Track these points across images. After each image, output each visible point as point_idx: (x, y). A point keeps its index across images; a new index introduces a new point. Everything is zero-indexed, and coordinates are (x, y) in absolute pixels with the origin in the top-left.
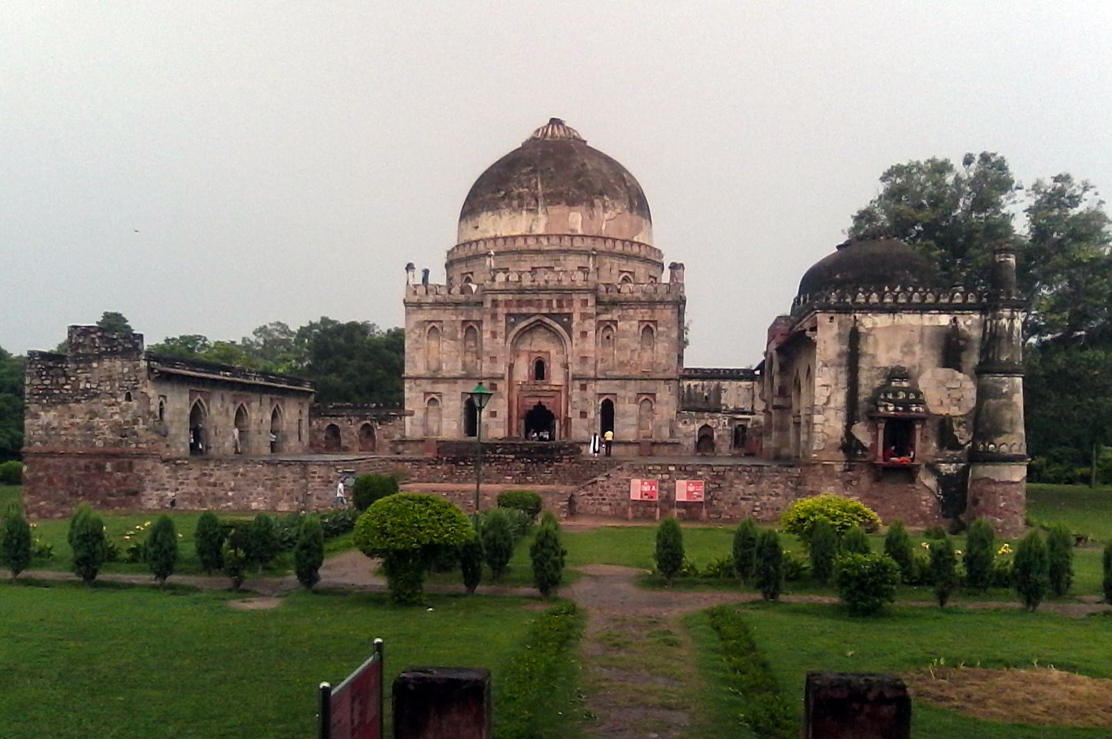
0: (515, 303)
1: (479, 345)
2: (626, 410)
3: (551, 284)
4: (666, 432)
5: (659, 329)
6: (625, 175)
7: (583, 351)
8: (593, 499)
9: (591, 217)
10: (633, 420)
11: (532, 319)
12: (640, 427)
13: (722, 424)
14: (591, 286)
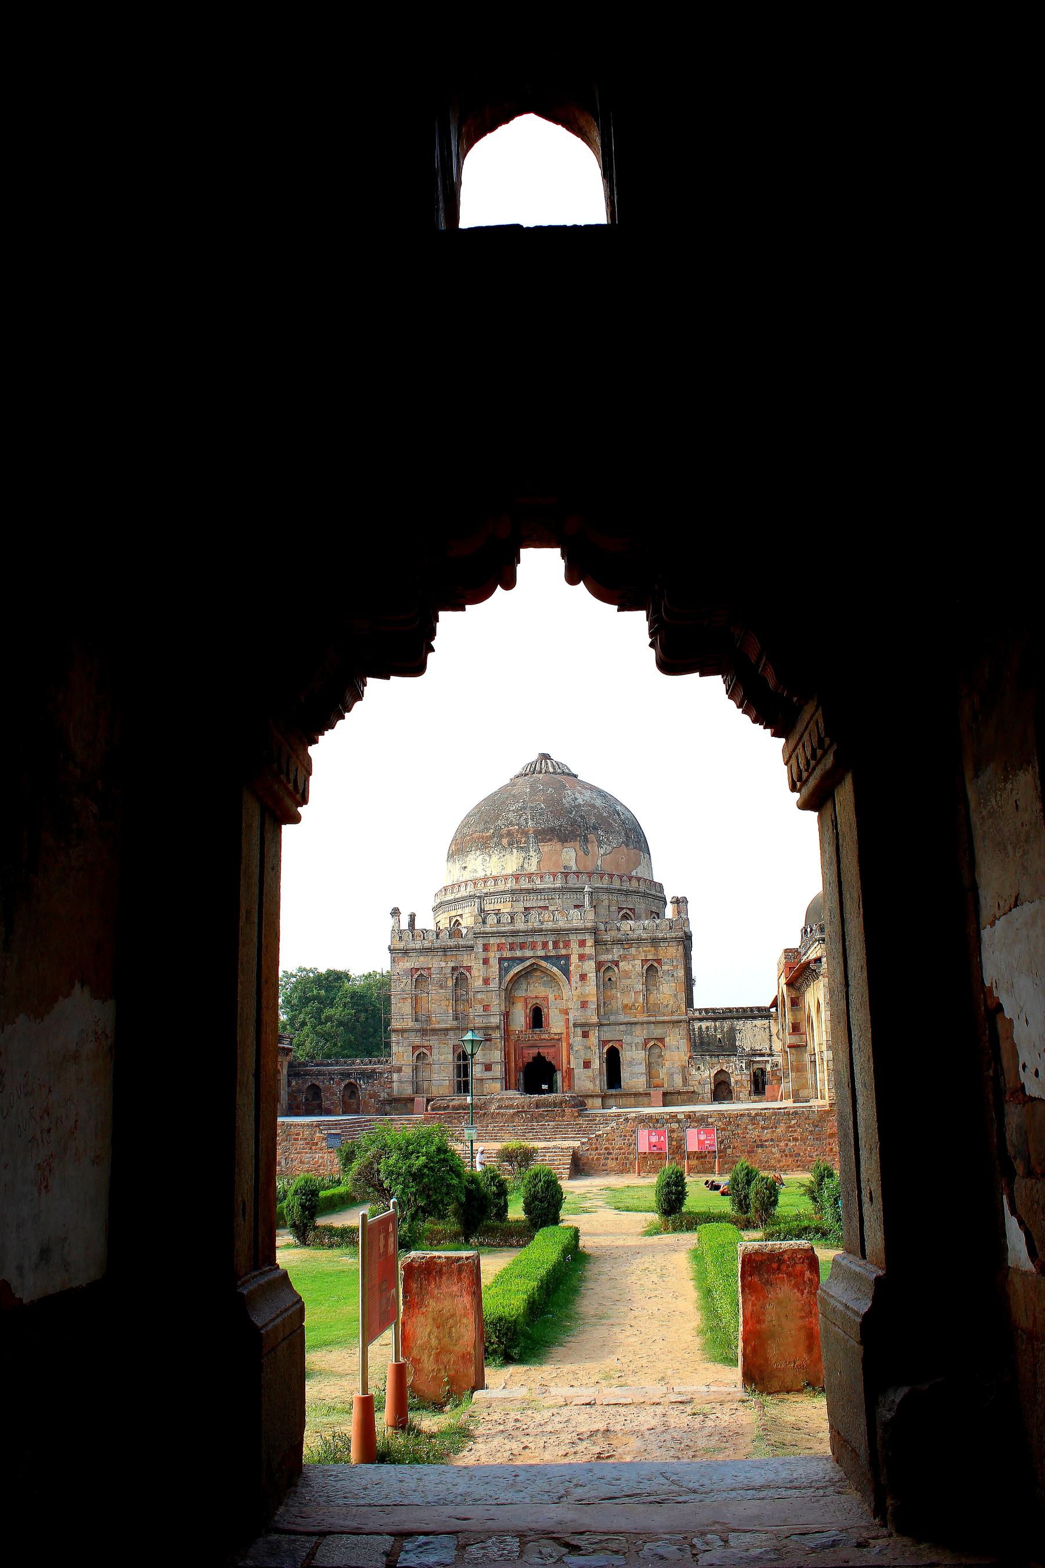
1: (471, 994)
3: (549, 925)
4: (678, 1080)
5: (665, 968)
6: (618, 808)
8: (599, 1154)
9: (586, 853)
10: (642, 1069)
11: (528, 963)
12: (650, 1074)
14: (589, 925)
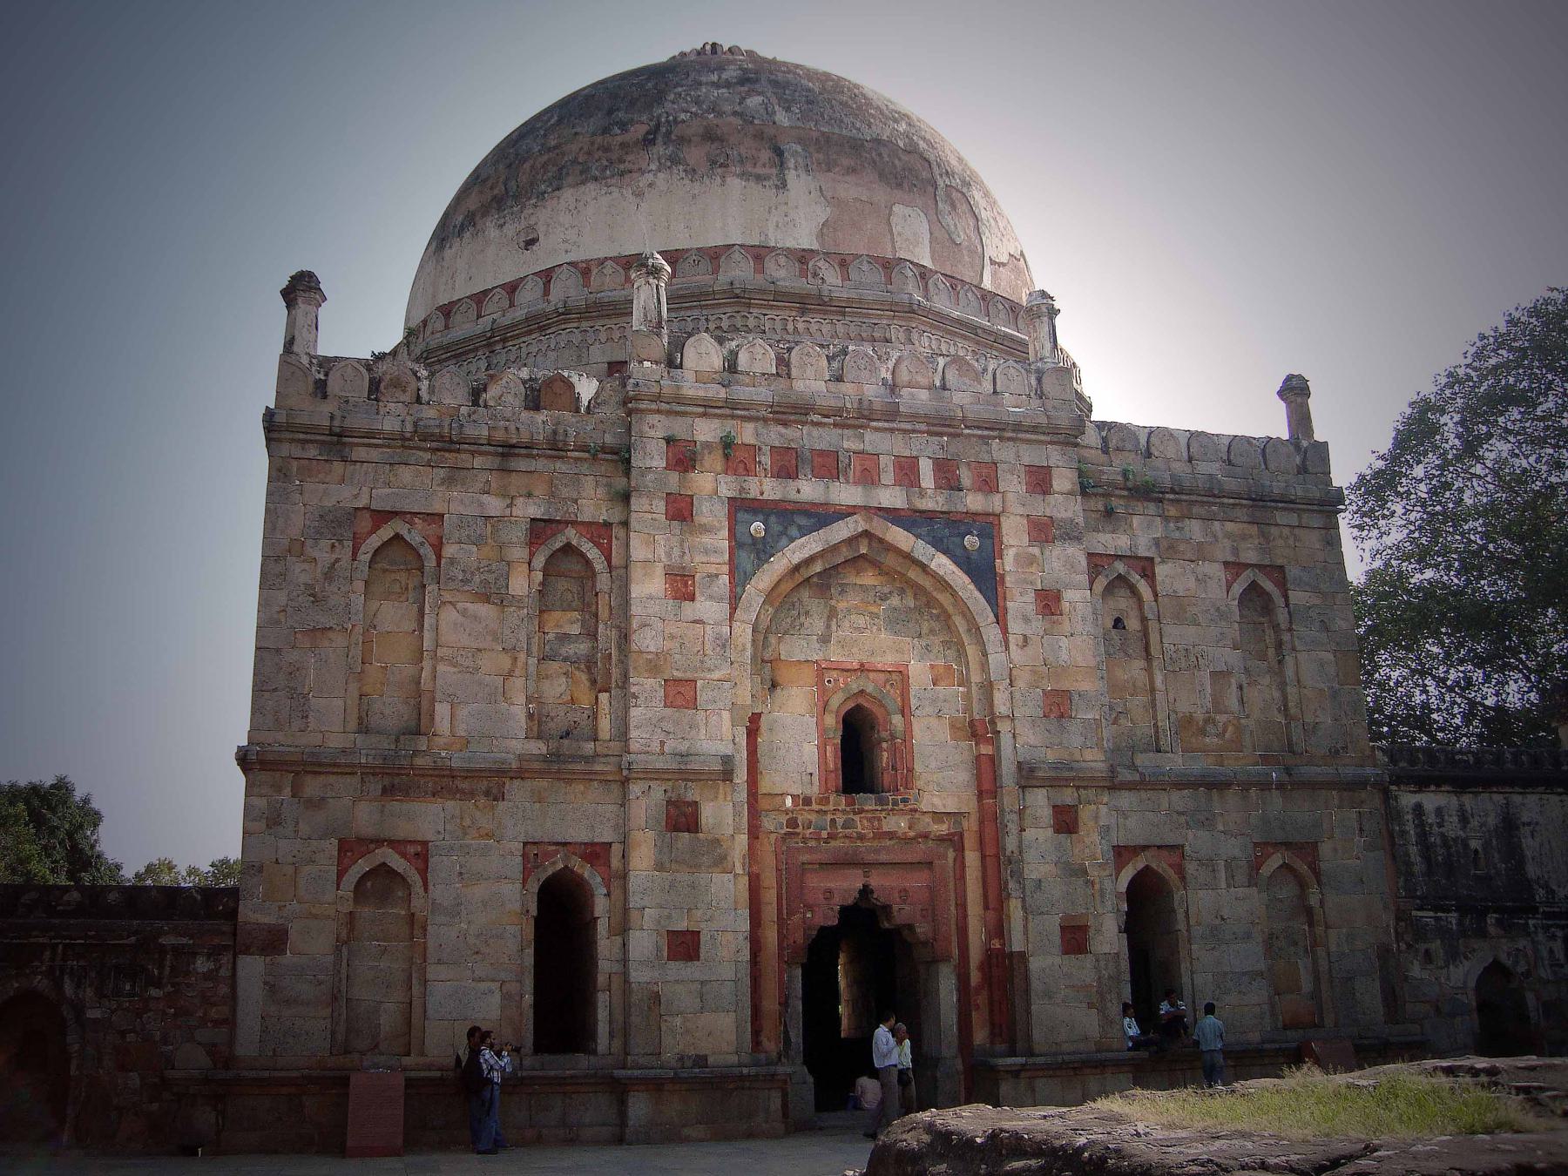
0: (766, 459)
1: (607, 634)
2: (1221, 912)
3: (918, 398)
4: (1369, 995)
5: (1296, 597)
7: (1052, 668)
11: (841, 531)
13: (1545, 954)
14: (1063, 419)
